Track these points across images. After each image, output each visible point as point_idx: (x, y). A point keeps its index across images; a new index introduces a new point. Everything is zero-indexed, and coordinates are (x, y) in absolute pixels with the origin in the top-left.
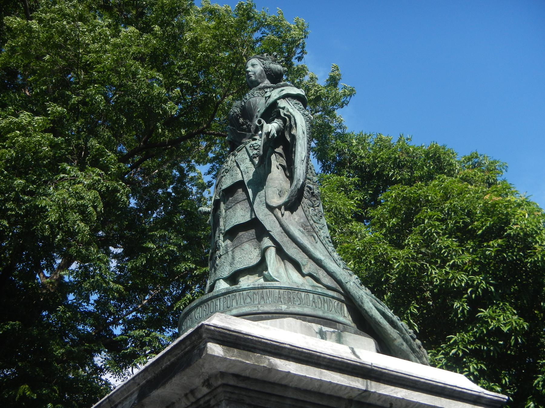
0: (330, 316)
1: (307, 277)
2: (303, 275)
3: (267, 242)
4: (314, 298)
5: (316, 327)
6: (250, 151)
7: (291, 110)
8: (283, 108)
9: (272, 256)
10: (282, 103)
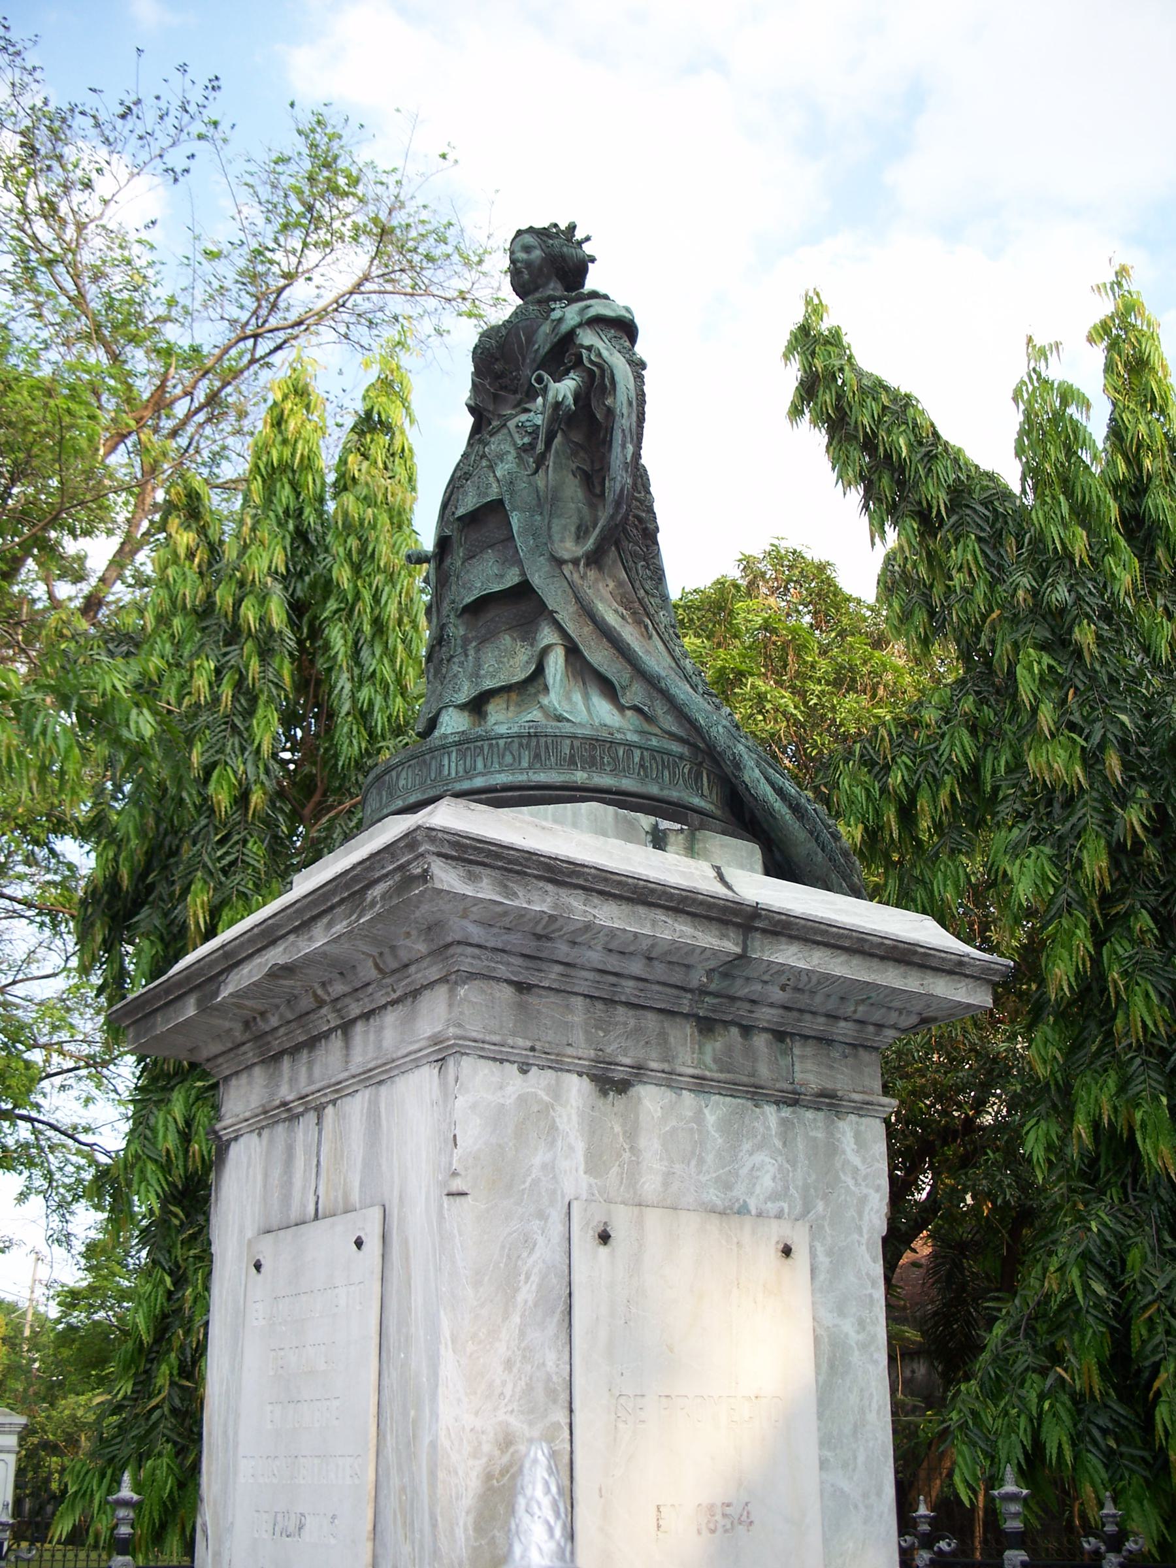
0: (674, 794)
1: (629, 713)
2: (621, 708)
3: (547, 636)
4: (642, 758)
5: (646, 821)
6: (516, 436)
7: (605, 353)
8: (589, 348)
10: (587, 338)
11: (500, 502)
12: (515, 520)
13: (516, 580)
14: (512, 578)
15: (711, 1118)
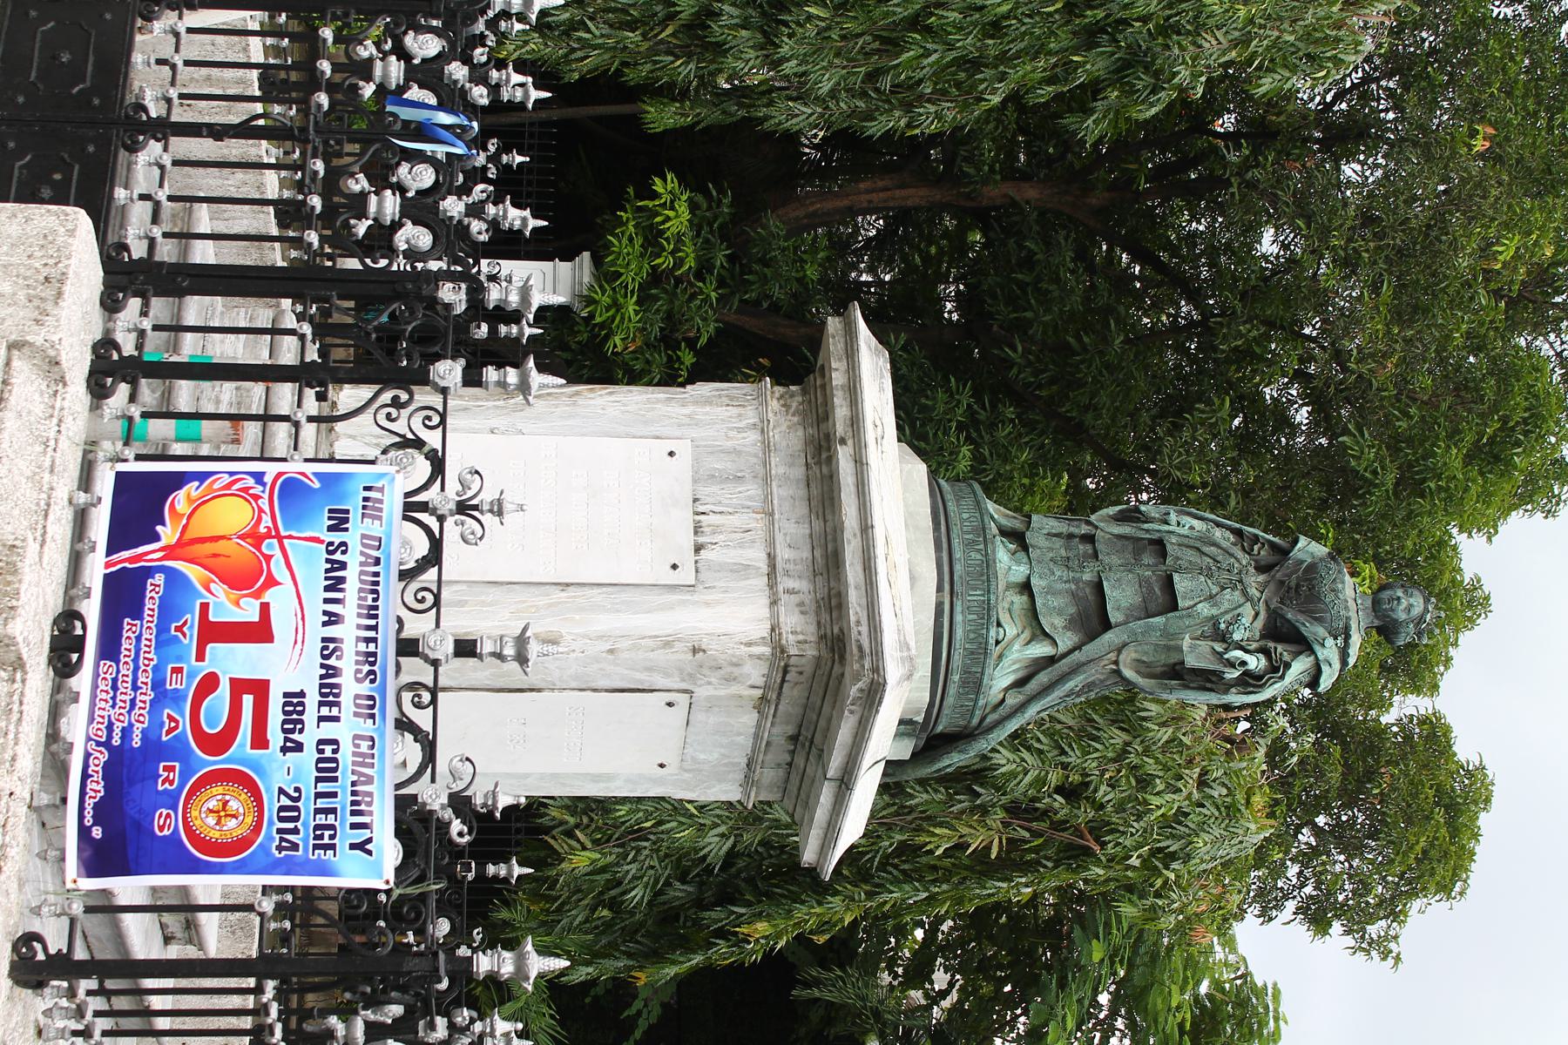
2: (1007, 689)
5: (920, 719)
9: (1041, 649)
11: (1175, 607)
12: (1158, 620)
13: (1113, 620)
14: (1114, 616)
15: (740, 739)
